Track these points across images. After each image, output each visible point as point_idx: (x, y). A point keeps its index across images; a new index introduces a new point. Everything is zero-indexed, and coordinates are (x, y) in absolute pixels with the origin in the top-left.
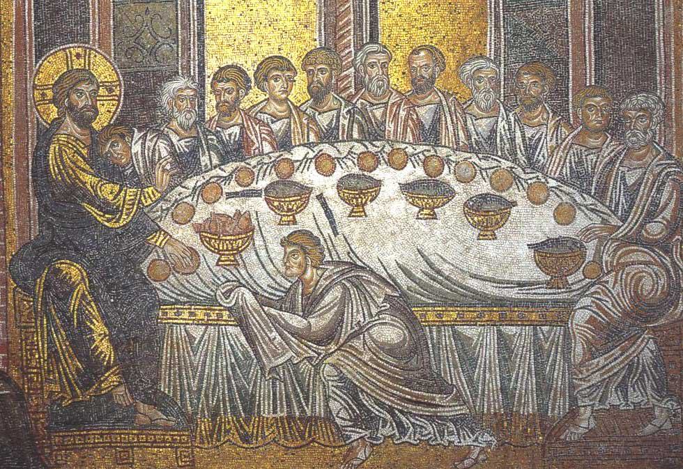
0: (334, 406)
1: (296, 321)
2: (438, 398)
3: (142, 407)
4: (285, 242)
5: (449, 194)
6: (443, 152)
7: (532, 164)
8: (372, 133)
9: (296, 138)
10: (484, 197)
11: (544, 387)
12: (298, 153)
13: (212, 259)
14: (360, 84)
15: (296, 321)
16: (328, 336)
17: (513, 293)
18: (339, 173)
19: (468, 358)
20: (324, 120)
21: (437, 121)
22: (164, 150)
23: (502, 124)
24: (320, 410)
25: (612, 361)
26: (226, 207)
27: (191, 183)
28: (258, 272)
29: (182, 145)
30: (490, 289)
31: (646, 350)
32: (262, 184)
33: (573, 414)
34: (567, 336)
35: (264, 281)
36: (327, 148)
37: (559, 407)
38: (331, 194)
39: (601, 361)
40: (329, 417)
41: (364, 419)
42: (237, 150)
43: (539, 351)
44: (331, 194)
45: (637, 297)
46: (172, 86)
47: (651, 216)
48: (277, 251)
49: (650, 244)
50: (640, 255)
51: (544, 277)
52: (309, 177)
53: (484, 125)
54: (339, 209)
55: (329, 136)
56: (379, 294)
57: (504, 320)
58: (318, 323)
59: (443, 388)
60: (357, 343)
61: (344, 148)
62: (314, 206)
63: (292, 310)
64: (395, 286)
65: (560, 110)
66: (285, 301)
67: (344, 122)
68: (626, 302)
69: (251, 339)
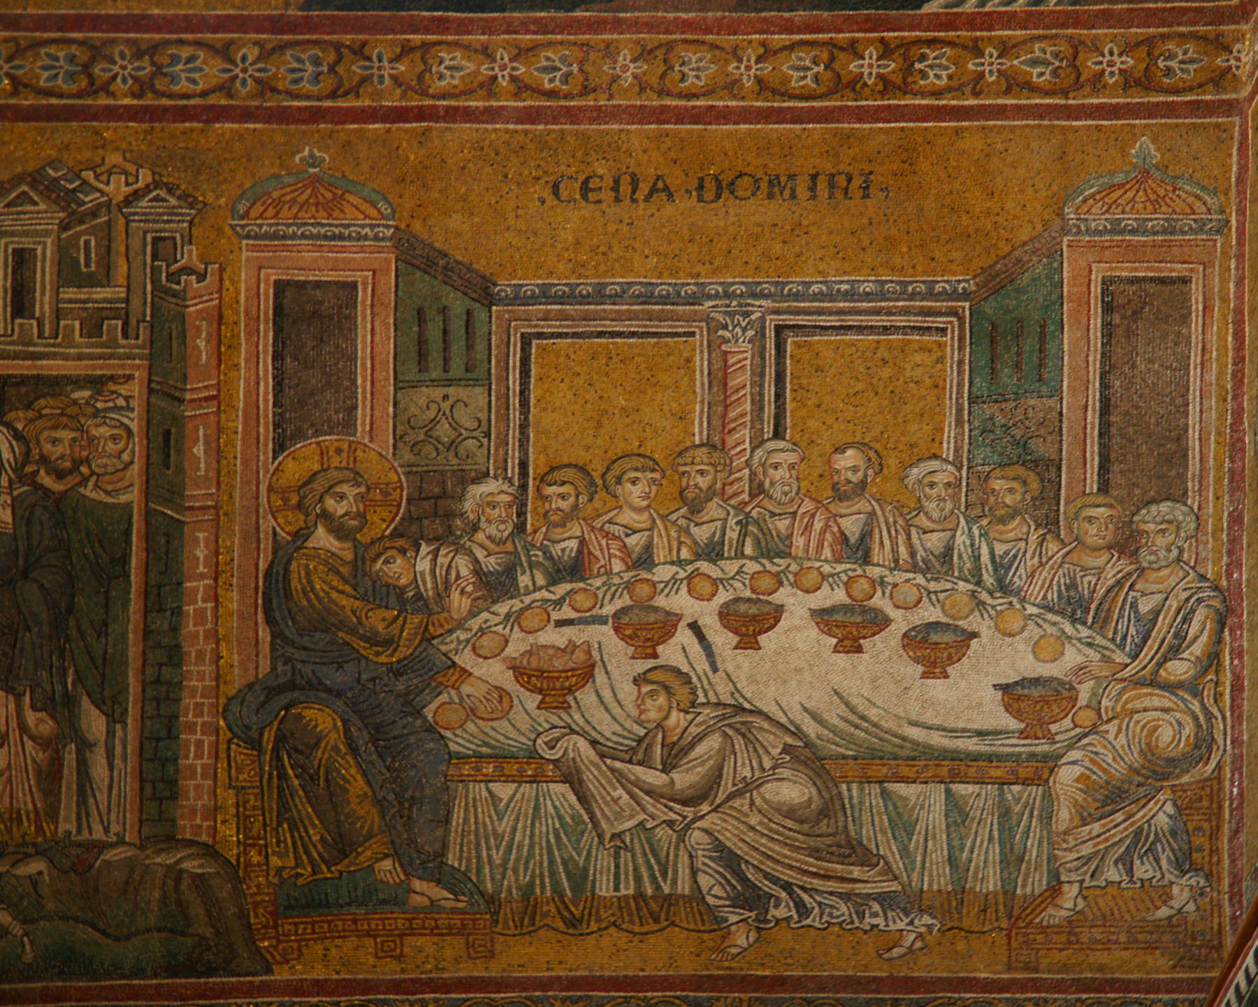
0: (704, 881)
1: (654, 778)
2: (856, 872)
3: (417, 885)
4: (636, 681)
5: (880, 622)
6: (875, 572)
7: (1003, 587)
8: (772, 548)
9: (660, 555)
10: (935, 626)
11: (1012, 860)
12: (663, 573)
13: (532, 701)
14: (758, 490)
15: (654, 778)
17: (971, 745)
18: (722, 597)
19: (902, 824)
20: (702, 534)
21: (866, 536)
22: (463, 565)
23: (961, 539)
24: (684, 887)
25: (1119, 827)
26: (553, 637)
27: (503, 608)
28: (599, 718)
29: (492, 564)
30: (937, 740)
32: (609, 610)
33: (1055, 889)
34: (1048, 797)
35: (607, 728)
36: (704, 566)
37: (1037, 883)
38: (710, 622)
39: (1096, 827)
42: (576, 569)
44: (710, 622)
45: (1149, 751)
46: (477, 491)
47: (1174, 651)
48: (627, 691)
49: (1171, 687)
50: (1159, 699)
51: (1014, 724)
52: (681, 602)
53: (935, 541)
54: (722, 639)
55: (713, 552)
56: (774, 743)
57: (956, 777)
58: (683, 779)
59: (867, 858)
60: (741, 803)
61: (731, 567)
62: (684, 636)
64: (798, 733)
65: (1050, 524)
66: (638, 752)
67: (732, 534)
68: (1135, 758)
69: (583, 799)
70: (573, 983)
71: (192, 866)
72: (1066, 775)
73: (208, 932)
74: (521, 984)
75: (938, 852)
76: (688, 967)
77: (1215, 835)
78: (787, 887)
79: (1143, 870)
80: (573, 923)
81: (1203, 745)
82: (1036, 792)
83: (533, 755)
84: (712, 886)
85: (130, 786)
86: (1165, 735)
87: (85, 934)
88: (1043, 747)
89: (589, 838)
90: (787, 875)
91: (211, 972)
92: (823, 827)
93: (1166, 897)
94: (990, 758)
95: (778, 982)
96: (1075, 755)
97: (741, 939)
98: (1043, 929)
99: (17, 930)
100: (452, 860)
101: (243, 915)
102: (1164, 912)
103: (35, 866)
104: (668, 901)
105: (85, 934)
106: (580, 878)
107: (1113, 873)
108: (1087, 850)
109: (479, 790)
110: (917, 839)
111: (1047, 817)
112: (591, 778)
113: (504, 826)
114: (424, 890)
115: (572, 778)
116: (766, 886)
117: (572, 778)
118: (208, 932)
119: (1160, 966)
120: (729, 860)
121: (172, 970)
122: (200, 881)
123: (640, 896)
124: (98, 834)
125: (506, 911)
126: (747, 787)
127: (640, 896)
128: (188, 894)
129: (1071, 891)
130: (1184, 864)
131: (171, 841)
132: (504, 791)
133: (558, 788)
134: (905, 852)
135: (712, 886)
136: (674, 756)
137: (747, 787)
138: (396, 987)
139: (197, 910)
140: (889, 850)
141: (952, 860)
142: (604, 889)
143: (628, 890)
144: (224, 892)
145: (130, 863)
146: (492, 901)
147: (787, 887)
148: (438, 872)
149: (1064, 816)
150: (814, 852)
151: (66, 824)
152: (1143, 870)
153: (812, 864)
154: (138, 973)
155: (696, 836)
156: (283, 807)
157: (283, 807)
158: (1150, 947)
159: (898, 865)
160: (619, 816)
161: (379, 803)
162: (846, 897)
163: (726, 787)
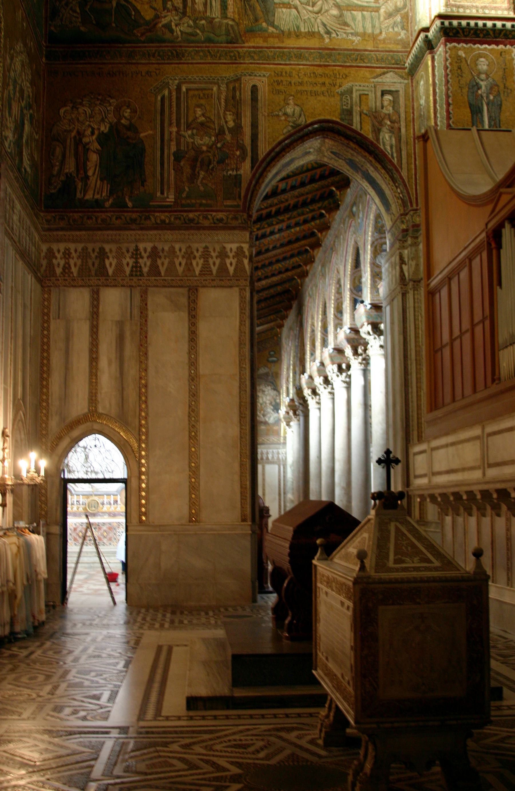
0: (320, 29)
1: (310, 8)
2: (346, 28)
3: (270, 28)
11: (373, 27)
15: (310, 8)
16: (317, 13)
17: (365, 4)
19: (354, 19)
24: (316, 30)
25: (391, 21)
31: (398, 18)
33: (381, 33)
34: (379, 15)
37: (377, 31)
39: (387, 21)
40: (319, 32)
41: (328, 33)
43: (372, 17)
57: (363, 10)
58: (316, 9)
60: (326, 14)
63: (309, 5)
68: (393, 8)
69: (298, 12)
70: (298, 48)
71: (231, 23)
72: (382, 11)
73: (233, 36)
74: (289, 48)
75: (361, 25)
76: (317, 46)
77: (408, 23)
78: (335, 31)
79: (396, 29)
80: (297, 36)
81: (405, 6)
82: (377, 14)
83: (289, 4)
84: (322, 31)
85: (219, 7)
86: (398, 4)
87: (212, 35)
88: (377, 5)
89: (299, 20)
90: (334, 28)
91: (234, 43)
92: (340, 19)
93: (400, 35)
94: (369, 7)
95: (334, 49)
96: (383, 7)
97: (327, 41)
98: (379, 40)
99: (200, 34)
100: (276, 23)
101: (239, 33)
102: (399, 38)
103: (203, 22)
104: (314, 33)
105: (212, 35)
106: (298, 27)
107: (391, 30)
108: (386, 25)
109: (280, 10)
110: (356, 23)
111: (379, 19)
112: (300, 8)
113: (284, 17)
114: (271, 29)
115: (296, 8)
116: (331, 30)
117: (296, 8)
118: (233, 36)
119: (399, 48)
120: (324, 25)
121: (227, 43)
122: (232, 26)
123: (309, 32)
124: (214, 16)
125: (285, 34)
126: (327, 11)
127: (309, 32)
128: (230, 28)
129: (384, 33)
130: (403, 28)
131: (226, 18)
132: (284, 10)
133: (294, 11)
134: (355, 24)
135: (322, 31)
136: (314, 5)
137: (327, 11)
138: (267, 48)
139: (231, 31)
140: (352, 24)
141: (363, 27)
142: (302, 30)
143: (307, 30)
144: (236, 28)
145: (220, 22)
146: (283, 32)
147: (335, 31)
148: (273, 26)
149: (382, 18)
150: (339, 24)
151: (208, 14)
152: (396, 29)
153: (339, 26)
154: (221, 43)
155: (318, 20)
156: (246, 12)
157: (246, 12)
158: (398, 44)
159: (354, 27)
160: (305, 16)
161: (263, 12)
162: (345, 33)
163: (323, 11)
